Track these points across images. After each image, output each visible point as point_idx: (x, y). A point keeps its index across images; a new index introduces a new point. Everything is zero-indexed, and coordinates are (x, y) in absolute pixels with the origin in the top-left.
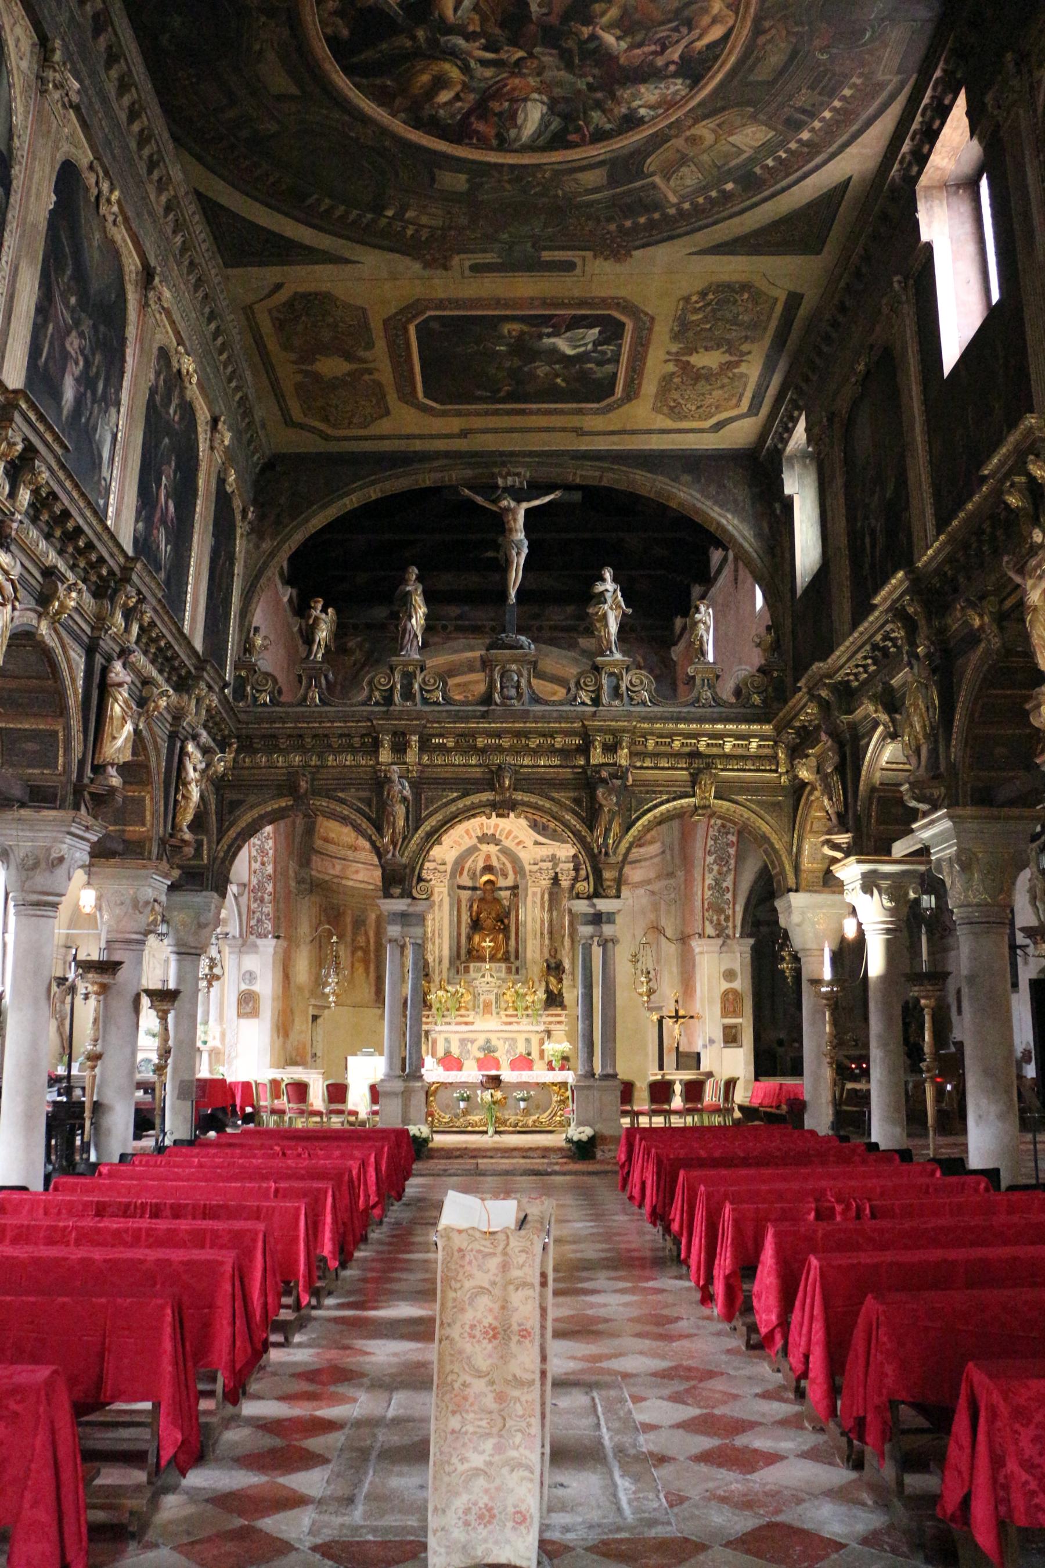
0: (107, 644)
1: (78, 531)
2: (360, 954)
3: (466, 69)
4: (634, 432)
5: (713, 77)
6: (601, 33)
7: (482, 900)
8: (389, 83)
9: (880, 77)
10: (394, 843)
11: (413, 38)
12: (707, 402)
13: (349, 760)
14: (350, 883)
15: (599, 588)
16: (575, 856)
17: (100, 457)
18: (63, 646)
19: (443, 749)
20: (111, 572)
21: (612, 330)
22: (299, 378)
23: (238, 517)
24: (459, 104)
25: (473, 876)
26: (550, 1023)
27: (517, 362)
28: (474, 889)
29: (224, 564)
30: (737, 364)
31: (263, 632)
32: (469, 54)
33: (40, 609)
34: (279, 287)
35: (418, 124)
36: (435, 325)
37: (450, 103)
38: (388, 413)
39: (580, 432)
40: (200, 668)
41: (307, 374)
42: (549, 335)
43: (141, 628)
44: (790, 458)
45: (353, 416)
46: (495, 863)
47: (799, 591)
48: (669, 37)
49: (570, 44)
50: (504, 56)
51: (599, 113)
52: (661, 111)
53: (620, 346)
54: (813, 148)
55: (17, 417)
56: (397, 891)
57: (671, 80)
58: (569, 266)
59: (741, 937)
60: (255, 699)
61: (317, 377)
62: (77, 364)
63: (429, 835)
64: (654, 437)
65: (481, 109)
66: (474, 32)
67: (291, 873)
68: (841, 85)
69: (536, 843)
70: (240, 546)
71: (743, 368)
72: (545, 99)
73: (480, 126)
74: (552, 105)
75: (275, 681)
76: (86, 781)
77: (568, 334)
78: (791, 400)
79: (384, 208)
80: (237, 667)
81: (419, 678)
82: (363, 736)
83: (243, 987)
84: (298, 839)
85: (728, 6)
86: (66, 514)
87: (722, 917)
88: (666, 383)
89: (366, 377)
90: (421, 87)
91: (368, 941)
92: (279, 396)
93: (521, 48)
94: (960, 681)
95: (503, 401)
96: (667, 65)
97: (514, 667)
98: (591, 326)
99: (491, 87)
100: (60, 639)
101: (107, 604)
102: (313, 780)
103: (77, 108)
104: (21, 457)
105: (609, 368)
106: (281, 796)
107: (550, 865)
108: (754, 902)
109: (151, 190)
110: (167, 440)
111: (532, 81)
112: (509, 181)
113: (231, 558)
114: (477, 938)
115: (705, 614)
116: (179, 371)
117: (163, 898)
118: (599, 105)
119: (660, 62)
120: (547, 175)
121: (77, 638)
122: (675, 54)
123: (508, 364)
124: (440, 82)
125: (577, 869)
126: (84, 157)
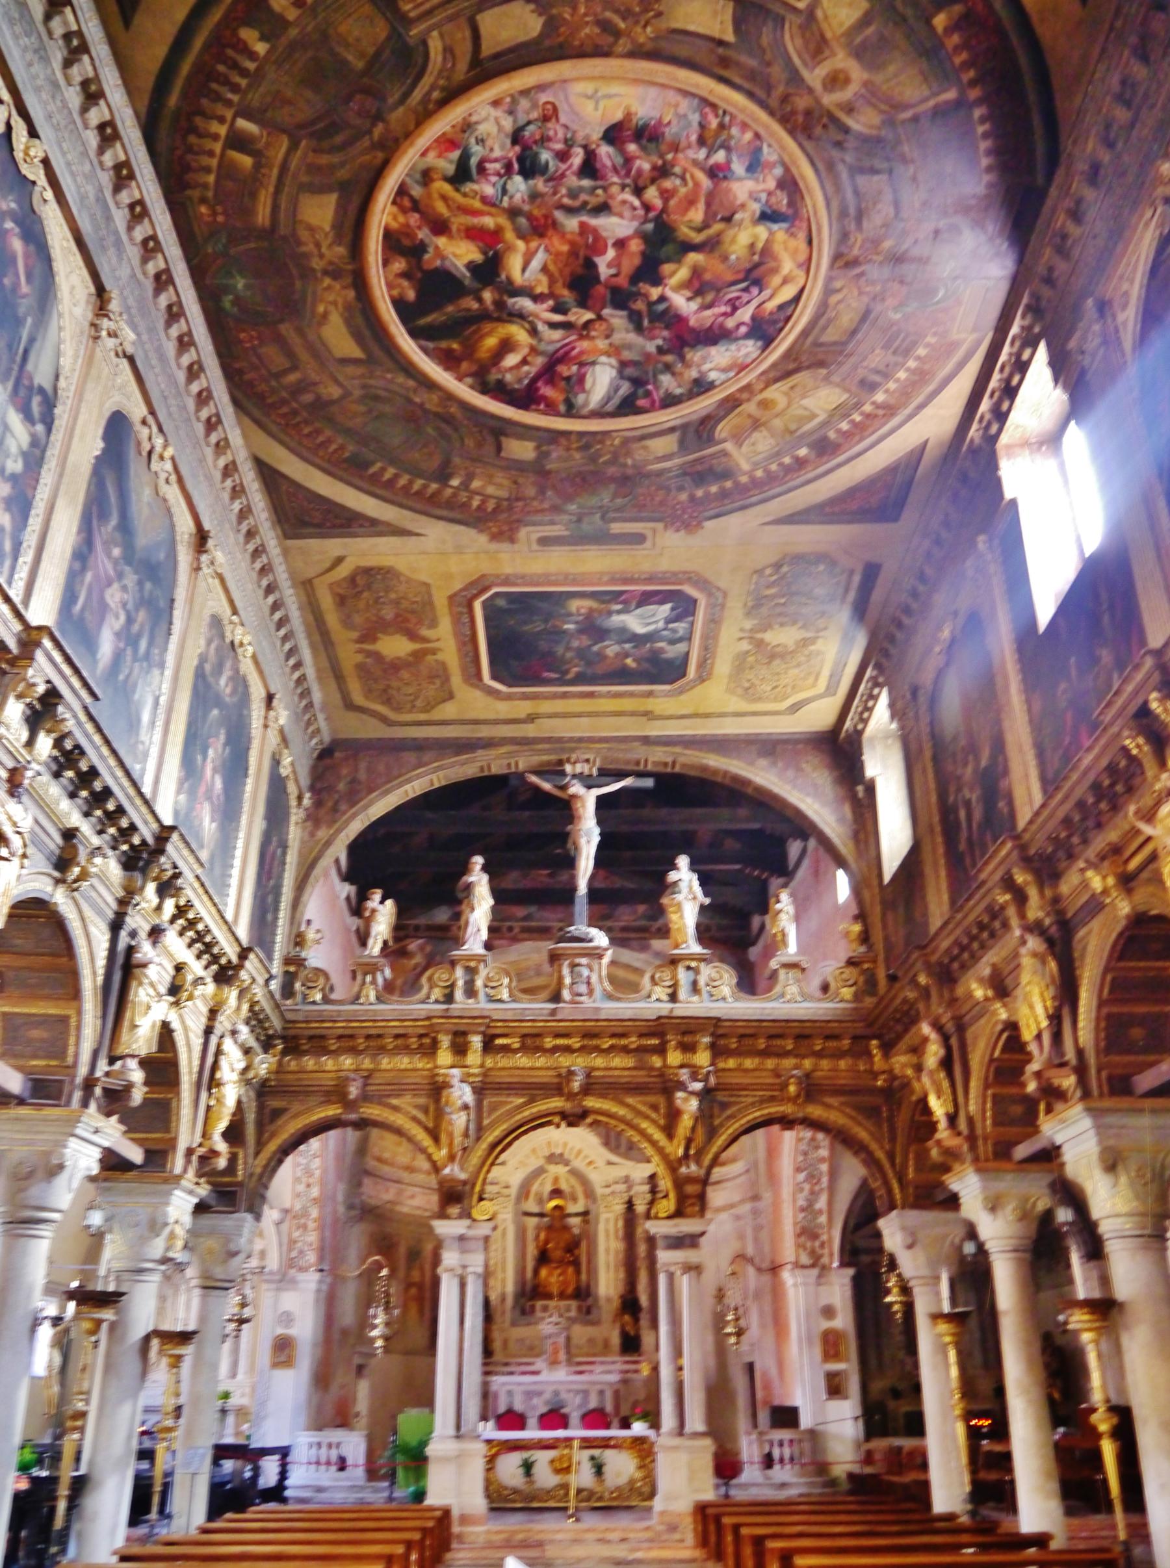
0: (137, 921)
1: (107, 792)
2: (413, 1291)
3: (533, 332)
4: (707, 716)
6: (669, 293)
7: (550, 1228)
8: (455, 346)
9: (954, 336)
10: (452, 1158)
11: (480, 300)
12: (783, 682)
13: (404, 1062)
14: (405, 1210)
15: (673, 876)
16: (653, 1177)
17: (139, 720)
18: (83, 919)
19: (506, 1049)
20: (144, 842)
21: (685, 607)
22: (359, 658)
23: (293, 802)
24: (526, 368)
25: (540, 1201)
26: (627, 1372)
27: (585, 641)
28: (541, 1215)
29: (274, 853)
30: (813, 640)
31: (315, 926)
32: (537, 316)
33: (57, 874)
34: (339, 560)
35: (484, 388)
36: (501, 603)
38: (451, 696)
39: (648, 715)
40: (244, 954)
41: (369, 654)
42: (619, 612)
43: (177, 907)
44: (872, 739)
45: (417, 698)
46: (564, 1186)
47: (887, 878)
48: (738, 298)
49: (640, 305)
50: (571, 318)
52: (732, 374)
53: (692, 624)
54: (889, 410)
55: (39, 655)
56: (454, 1210)
58: (639, 539)
59: (843, 1264)
60: (305, 996)
61: (378, 657)
62: (117, 617)
63: (493, 1146)
64: (728, 720)
65: (549, 373)
66: (542, 294)
67: (340, 1197)
68: (914, 344)
69: (609, 1163)
70: (294, 833)
71: (819, 645)
72: (613, 361)
73: (547, 391)
75: (327, 976)
76: (99, 1073)
77: (639, 611)
78: (871, 678)
79: (450, 476)
80: (288, 961)
81: (483, 972)
82: (421, 1036)
83: (280, 1331)
84: (348, 1159)
86: (93, 772)
87: (817, 1244)
88: (740, 664)
89: (430, 658)
90: (489, 350)
91: (423, 1275)
92: (339, 677)
94: (1083, 956)
95: (572, 682)
96: (738, 326)
97: (584, 961)
98: (662, 602)
99: (557, 351)
100: (80, 912)
101: (137, 875)
102: (365, 1085)
103: (131, 360)
104: (42, 699)
105: (681, 647)
106: (329, 1102)
107: (623, 1187)
108: (852, 1224)
109: (209, 452)
110: (215, 712)
111: (602, 344)
113: (284, 846)
114: (544, 1272)
115: (785, 903)
116: (232, 643)
117: (187, 1219)
118: (668, 368)
119: (730, 323)
120: (617, 442)
121: (100, 913)
122: (745, 314)
123: (575, 644)
124: (506, 346)
125: (653, 1191)
126: (137, 410)
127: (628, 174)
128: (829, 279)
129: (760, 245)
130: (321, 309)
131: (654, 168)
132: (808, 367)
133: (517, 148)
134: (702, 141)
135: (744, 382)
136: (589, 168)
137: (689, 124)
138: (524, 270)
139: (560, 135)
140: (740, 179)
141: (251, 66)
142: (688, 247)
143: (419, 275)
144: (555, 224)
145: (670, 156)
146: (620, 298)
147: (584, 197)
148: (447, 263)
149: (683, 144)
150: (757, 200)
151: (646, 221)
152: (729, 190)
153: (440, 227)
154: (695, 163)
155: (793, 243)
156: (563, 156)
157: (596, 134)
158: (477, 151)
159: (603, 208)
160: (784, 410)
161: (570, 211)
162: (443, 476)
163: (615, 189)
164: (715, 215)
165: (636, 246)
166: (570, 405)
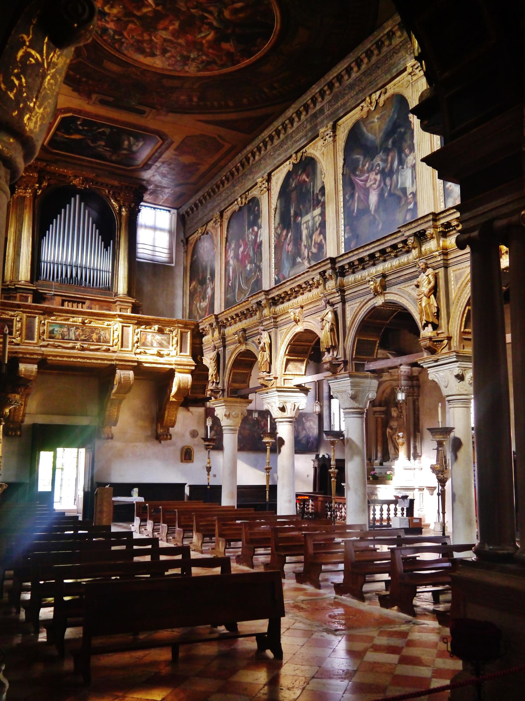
3: (221, 13)
6: (153, 5)
32: (215, 19)
50: (200, 13)
124: (235, 12)
136: (164, 51)
138: (208, 35)
140: (111, 29)
142: (139, 18)
150: (106, 20)
153: (229, 54)
156: (173, 56)
161: (180, 44)
163: (159, 44)
165: (161, 26)
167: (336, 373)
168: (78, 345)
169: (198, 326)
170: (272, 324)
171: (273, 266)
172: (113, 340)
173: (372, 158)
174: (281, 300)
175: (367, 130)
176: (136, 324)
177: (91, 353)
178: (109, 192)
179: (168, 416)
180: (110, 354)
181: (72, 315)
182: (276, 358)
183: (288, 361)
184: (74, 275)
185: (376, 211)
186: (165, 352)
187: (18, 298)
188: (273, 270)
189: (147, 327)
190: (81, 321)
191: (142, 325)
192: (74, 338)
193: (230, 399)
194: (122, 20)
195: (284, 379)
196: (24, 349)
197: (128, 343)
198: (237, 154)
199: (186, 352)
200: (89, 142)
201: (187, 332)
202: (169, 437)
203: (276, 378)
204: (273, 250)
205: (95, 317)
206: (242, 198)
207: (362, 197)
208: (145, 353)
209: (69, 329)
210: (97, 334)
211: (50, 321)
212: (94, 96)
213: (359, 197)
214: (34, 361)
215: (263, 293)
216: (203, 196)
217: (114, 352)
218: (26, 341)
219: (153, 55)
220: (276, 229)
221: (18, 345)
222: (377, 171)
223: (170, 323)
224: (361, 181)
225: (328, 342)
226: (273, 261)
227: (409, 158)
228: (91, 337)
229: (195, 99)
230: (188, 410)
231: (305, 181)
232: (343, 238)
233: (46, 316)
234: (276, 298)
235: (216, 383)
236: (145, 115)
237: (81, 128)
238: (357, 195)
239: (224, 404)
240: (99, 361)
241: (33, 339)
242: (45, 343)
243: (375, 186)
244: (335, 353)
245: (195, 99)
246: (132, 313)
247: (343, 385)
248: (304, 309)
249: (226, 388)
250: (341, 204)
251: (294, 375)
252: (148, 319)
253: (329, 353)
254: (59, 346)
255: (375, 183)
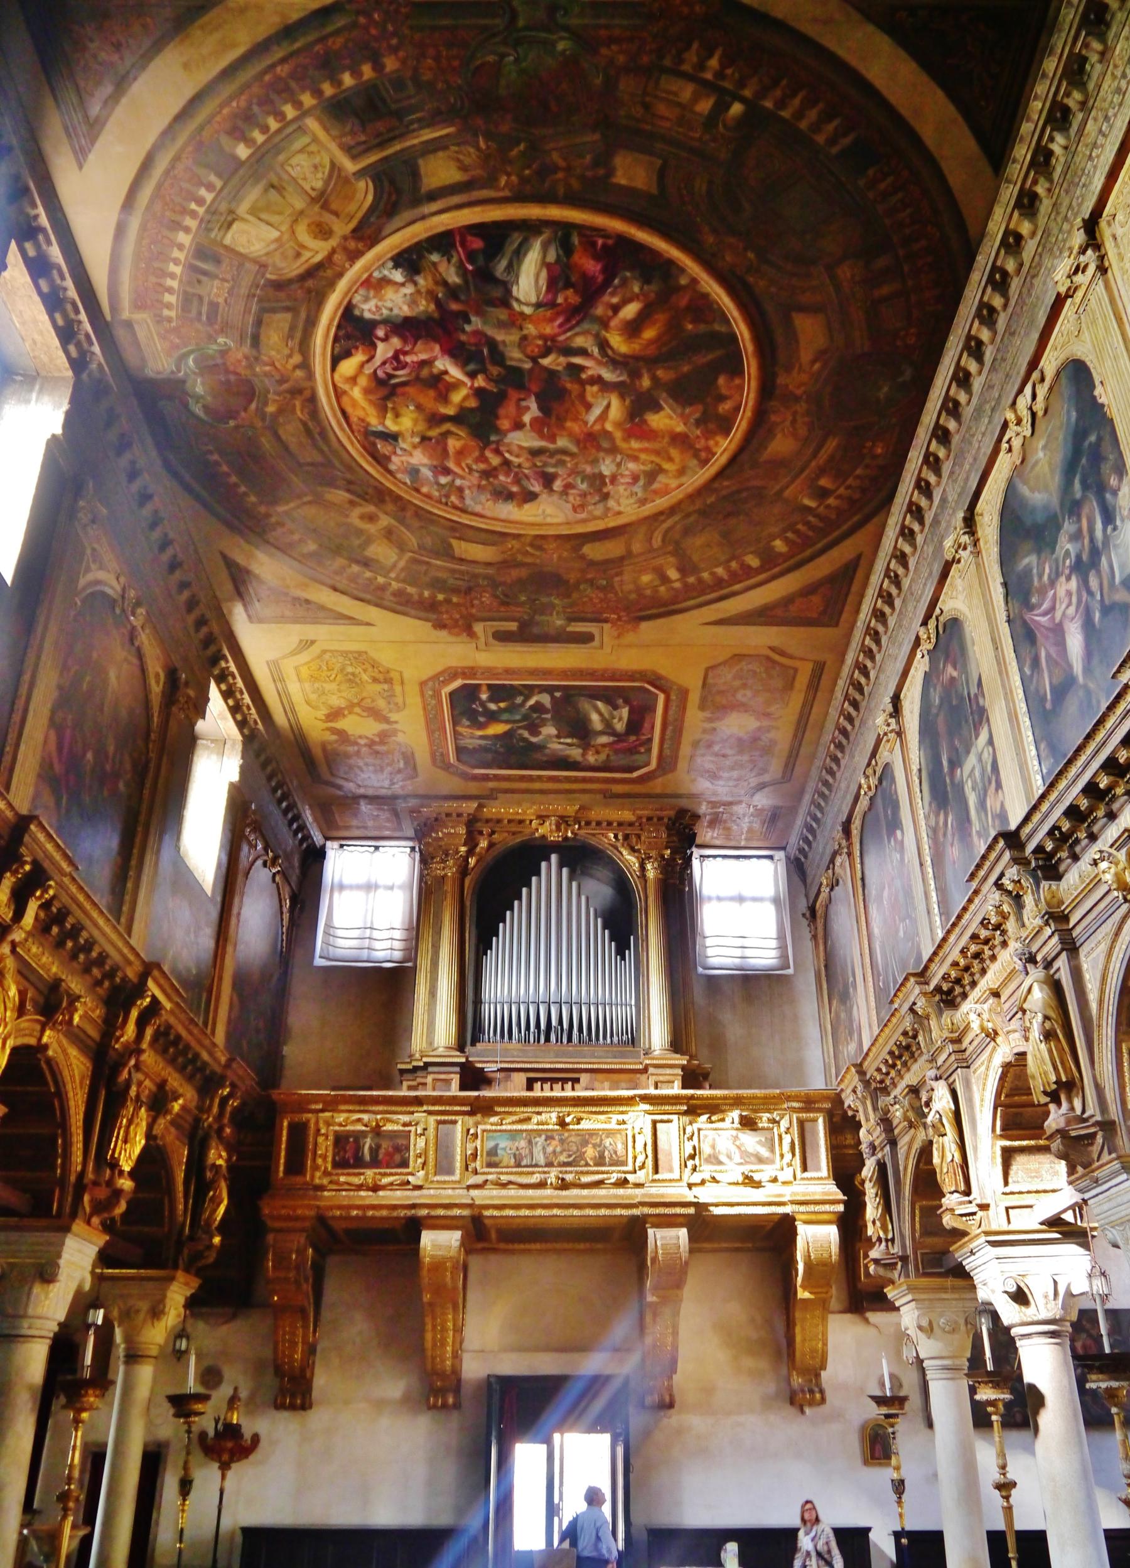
1: (1091, 789)
3: (603, 345)
5: (332, 320)
6: (465, 379)
8: (690, 327)
11: (654, 379)
32: (599, 363)
35: (669, 267)
37: (625, 302)
48: (395, 369)
49: (495, 370)
51: (450, 280)
57: (377, 317)
65: (590, 292)
72: (515, 305)
73: (592, 267)
74: (505, 300)
79: (743, 121)
85: (345, 392)
93: (545, 369)
99: (578, 324)
111: (531, 329)
112: (556, 169)
118: (453, 292)
119: (396, 342)
122: (383, 351)
124: (633, 329)
127: (516, 474)
128: (310, 376)
129: (389, 415)
130: (817, 366)
131: (496, 477)
132: (290, 281)
133: (605, 490)
134: (460, 490)
135: (360, 264)
136: (548, 480)
137: (473, 499)
138: (608, 406)
139: (571, 498)
140: (424, 465)
141: (789, 535)
142: (456, 419)
143: (709, 400)
144: (578, 442)
145: (484, 482)
146: (514, 379)
147: (553, 461)
148: (679, 411)
149: (475, 490)
151: (498, 443)
152: (431, 457)
153: (680, 440)
154: (462, 478)
155: (361, 414)
156: (568, 486)
157: (544, 497)
158: (638, 489)
159: (535, 453)
160: (296, 221)
161: (564, 452)
162: (754, 114)
164: (438, 442)
165: (505, 424)
166: (566, 248)
167: (1090, 1164)
168: (552, 1177)
169: (842, 1102)
170: (953, 1057)
171: (936, 911)
172: (635, 1158)
173: (1052, 545)
174: (958, 990)
175: (1032, 490)
176: (685, 1113)
177: (585, 1192)
178: (616, 837)
179: (804, 1340)
180: (629, 1192)
181: (537, 1109)
182: (975, 1149)
183: (1008, 1156)
184: (554, 1022)
185: (1088, 669)
186: (763, 1174)
187: (429, 1086)
188: (937, 919)
189: (714, 1118)
190: (554, 1120)
191: (700, 1115)
192: (540, 1159)
193: (925, 1281)
194: (430, 439)
195: (1007, 1209)
196: (431, 1196)
197: (671, 1160)
198: (835, 684)
199: (818, 1169)
200: (526, 734)
201: (815, 1120)
202: (818, 1396)
203: (984, 1207)
204: (930, 870)
205: (587, 1109)
206: (867, 777)
207: (1053, 651)
208: (714, 1180)
209: (530, 1142)
210: (594, 1146)
211: (489, 1127)
212: (478, 628)
213: (1048, 655)
214: (454, 1222)
215: (912, 980)
216: (813, 802)
217: (639, 1185)
218: (438, 1178)
219: (530, 497)
220: (927, 817)
221: (419, 1188)
222: (1067, 571)
223: (769, 1104)
224: (1045, 614)
225: (1045, 1073)
226: (935, 899)
227: (1120, 494)
228: (582, 1156)
229: (673, 574)
230: (867, 1320)
231: (952, 679)
232: (1039, 777)
233: (479, 1117)
234: (945, 987)
235: (887, 1240)
236: (596, 643)
237: (492, 706)
238: (1043, 654)
239: (909, 1297)
240: (603, 1212)
241: (450, 1172)
242: (479, 1179)
243: (1071, 610)
244: (1077, 1103)
245: (673, 574)
246: (684, 1087)
247: (1119, 1200)
248: (1003, 998)
249: (909, 1252)
250: (1020, 694)
251: (1037, 1192)
252: (713, 1098)
253: (1059, 1104)
254: (510, 1183)
255: (1069, 604)
